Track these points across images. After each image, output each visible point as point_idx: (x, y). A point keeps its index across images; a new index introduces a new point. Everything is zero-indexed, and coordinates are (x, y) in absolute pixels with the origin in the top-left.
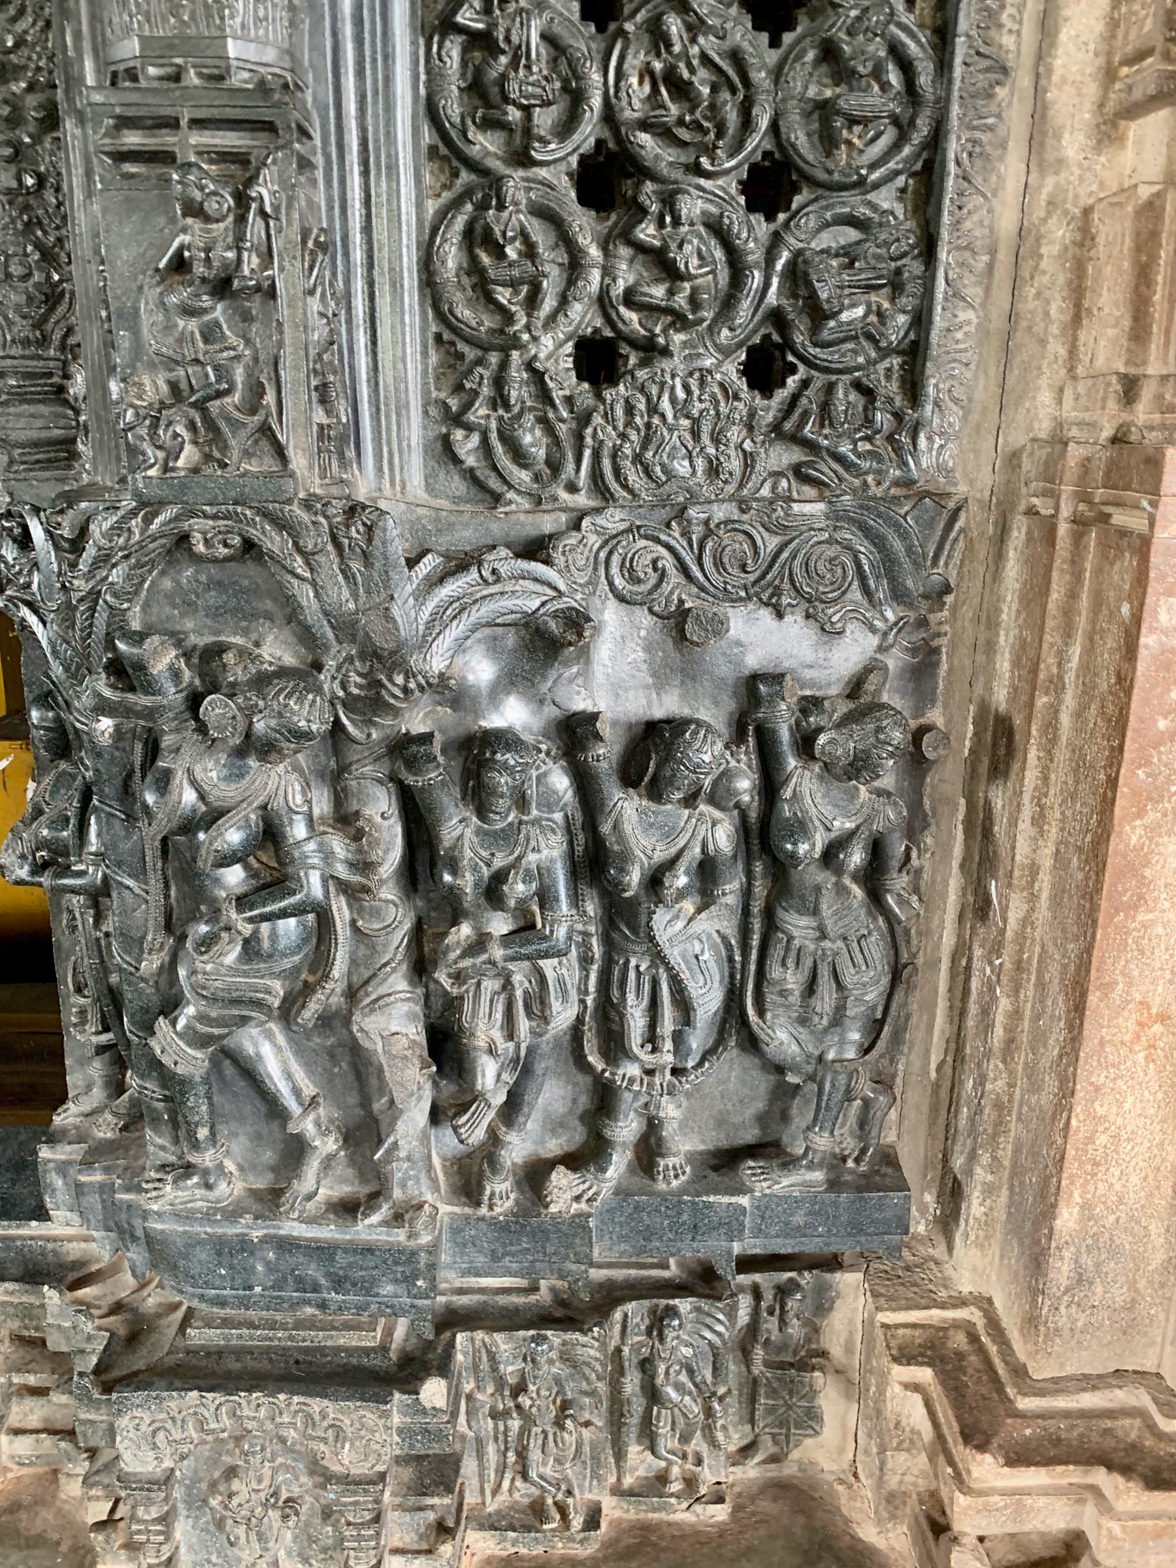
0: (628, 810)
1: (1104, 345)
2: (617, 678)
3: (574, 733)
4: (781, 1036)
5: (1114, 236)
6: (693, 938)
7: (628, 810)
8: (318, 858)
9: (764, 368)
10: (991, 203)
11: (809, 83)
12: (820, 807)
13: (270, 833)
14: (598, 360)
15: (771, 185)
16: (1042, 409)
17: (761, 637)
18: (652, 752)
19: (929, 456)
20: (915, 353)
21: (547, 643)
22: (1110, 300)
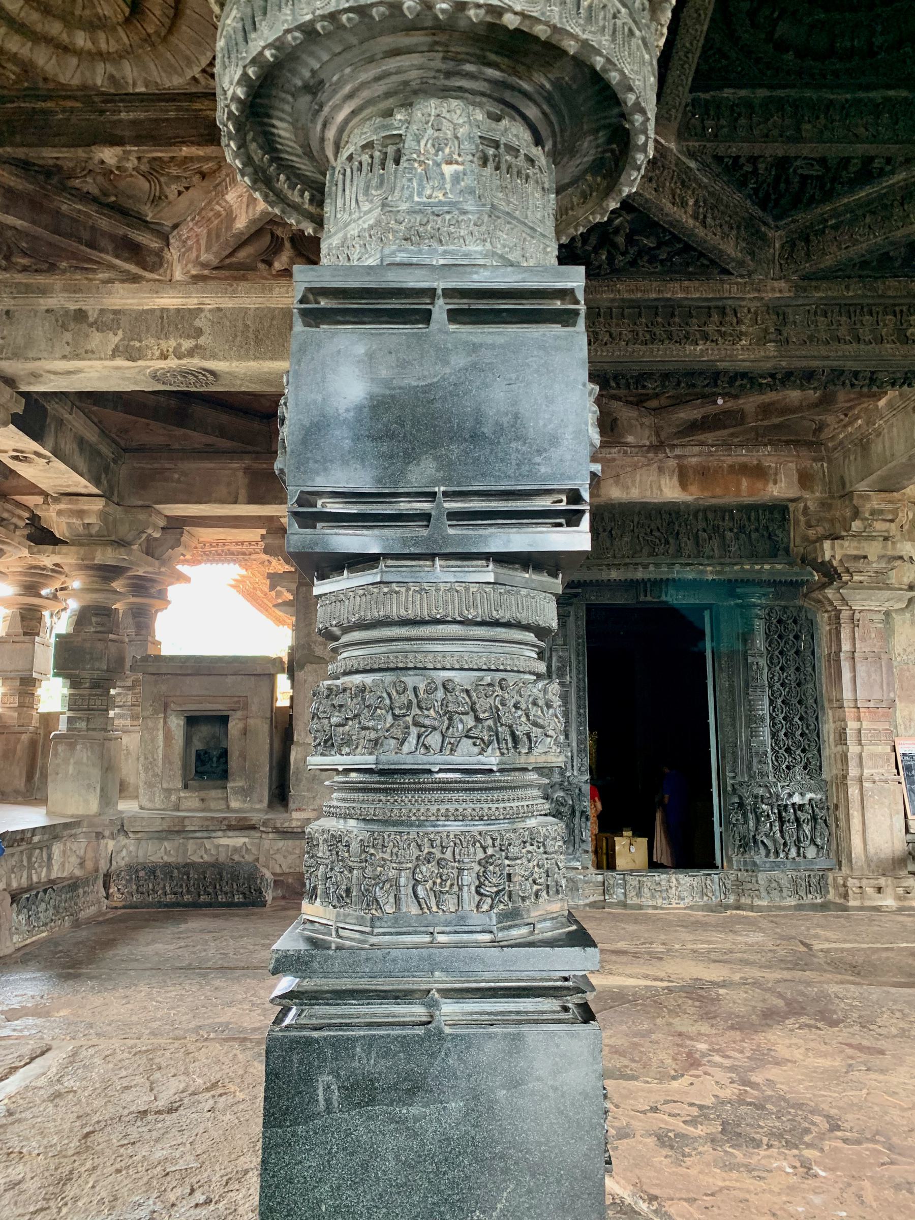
0: (799, 813)
1: (839, 766)
2: (797, 799)
3: (793, 804)
4: (818, 841)
5: (838, 756)
6: (807, 829)
7: (799, 813)
8: (773, 817)
9: (805, 768)
10: (825, 753)
11: (806, 742)
12: (820, 814)
13: (768, 815)
14: (788, 767)
15: (804, 751)
16: (834, 772)
17: (809, 795)
18: (801, 807)
19: (823, 777)
20: (820, 767)
21: (790, 795)
22: (839, 761)
